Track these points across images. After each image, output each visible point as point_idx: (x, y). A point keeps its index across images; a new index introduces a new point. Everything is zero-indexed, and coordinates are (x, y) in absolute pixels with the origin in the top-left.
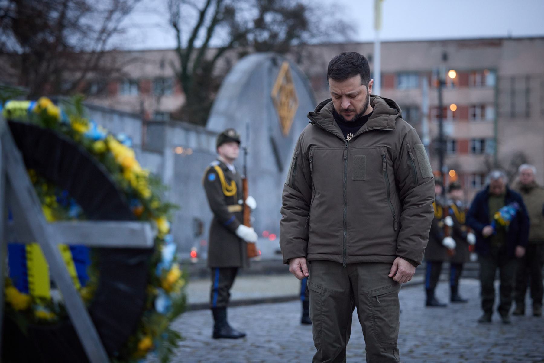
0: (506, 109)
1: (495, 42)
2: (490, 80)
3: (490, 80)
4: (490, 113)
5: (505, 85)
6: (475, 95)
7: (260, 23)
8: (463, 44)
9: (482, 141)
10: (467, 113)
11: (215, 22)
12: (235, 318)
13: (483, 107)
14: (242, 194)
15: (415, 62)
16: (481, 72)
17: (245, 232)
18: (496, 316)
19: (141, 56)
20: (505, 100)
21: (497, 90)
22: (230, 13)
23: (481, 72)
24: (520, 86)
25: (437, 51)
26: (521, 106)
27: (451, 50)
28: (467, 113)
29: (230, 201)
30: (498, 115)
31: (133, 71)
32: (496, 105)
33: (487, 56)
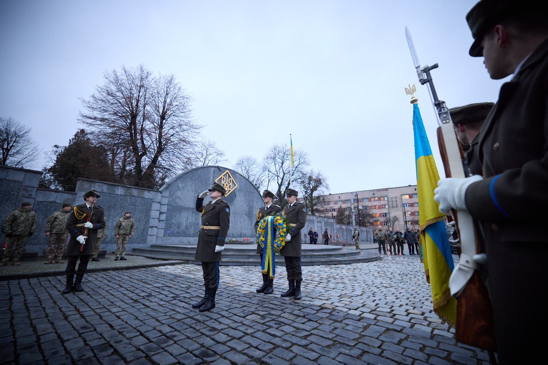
0: (391, 205)
1: (387, 189)
2: (386, 199)
3: (386, 199)
4: (387, 207)
5: (390, 200)
6: (382, 203)
8: (378, 190)
9: (386, 214)
13: (385, 205)
15: (366, 196)
16: (384, 197)
20: (390, 203)
23: (384, 197)
24: (394, 200)
25: (372, 193)
26: (395, 205)
27: (375, 192)
32: (388, 205)
33: (384, 193)
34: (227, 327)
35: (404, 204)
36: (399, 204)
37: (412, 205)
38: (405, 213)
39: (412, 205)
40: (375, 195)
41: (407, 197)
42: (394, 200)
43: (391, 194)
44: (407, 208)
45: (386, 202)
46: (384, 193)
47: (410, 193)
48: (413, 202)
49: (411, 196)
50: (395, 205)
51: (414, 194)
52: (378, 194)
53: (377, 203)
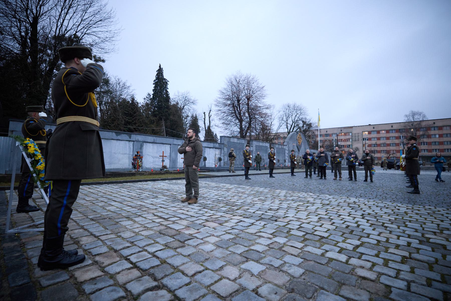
0: (354, 139)
1: (351, 127)
2: (351, 134)
3: (351, 134)
4: (351, 140)
5: (354, 135)
6: (347, 137)
7: (303, 127)
8: (345, 128)
10: (348, 140)
11: (294, 127)
12: (273, 175)
14: (249, 155)
15: (335, 132)
16: (349, 133)
17: (249, 161)
18: (309, 177)
19: (283, 133)
20: (354, 138)
21: (352, 136)
22: (298, 125)
23: (349, 133)
24: (357, 135)
25: (340, 129)
26: (357, 138)
27: (342, 129)
28: (348, 140)
29: (247, 156)
30: (352, 140)
31: (282, 135)
32: (352, 139)
33: (349, 130)
34: (224, 233)
35: (364, 139)
36: (361, 139)
37: (369, 139)
38: (364, 145)
39: (369, 139)
40: (342, 131)
41: (367, 133)
42: (357, 135)
43: (354, 131)
44: (367, 142)
45: (350, 137)
46: (349, 130)
47: (369, 130)
48: (371, 137)
49: (370, 133)
50: (357, 138)
51: (372, 131)
52: (345, 131)
53: (343, 138)
